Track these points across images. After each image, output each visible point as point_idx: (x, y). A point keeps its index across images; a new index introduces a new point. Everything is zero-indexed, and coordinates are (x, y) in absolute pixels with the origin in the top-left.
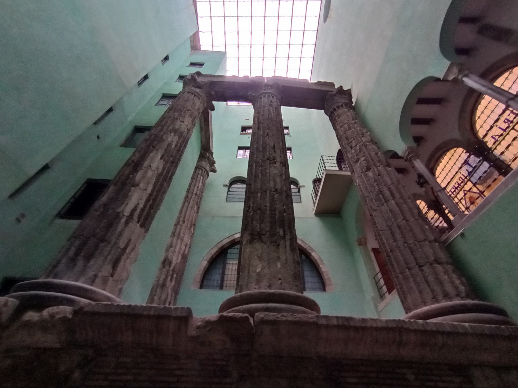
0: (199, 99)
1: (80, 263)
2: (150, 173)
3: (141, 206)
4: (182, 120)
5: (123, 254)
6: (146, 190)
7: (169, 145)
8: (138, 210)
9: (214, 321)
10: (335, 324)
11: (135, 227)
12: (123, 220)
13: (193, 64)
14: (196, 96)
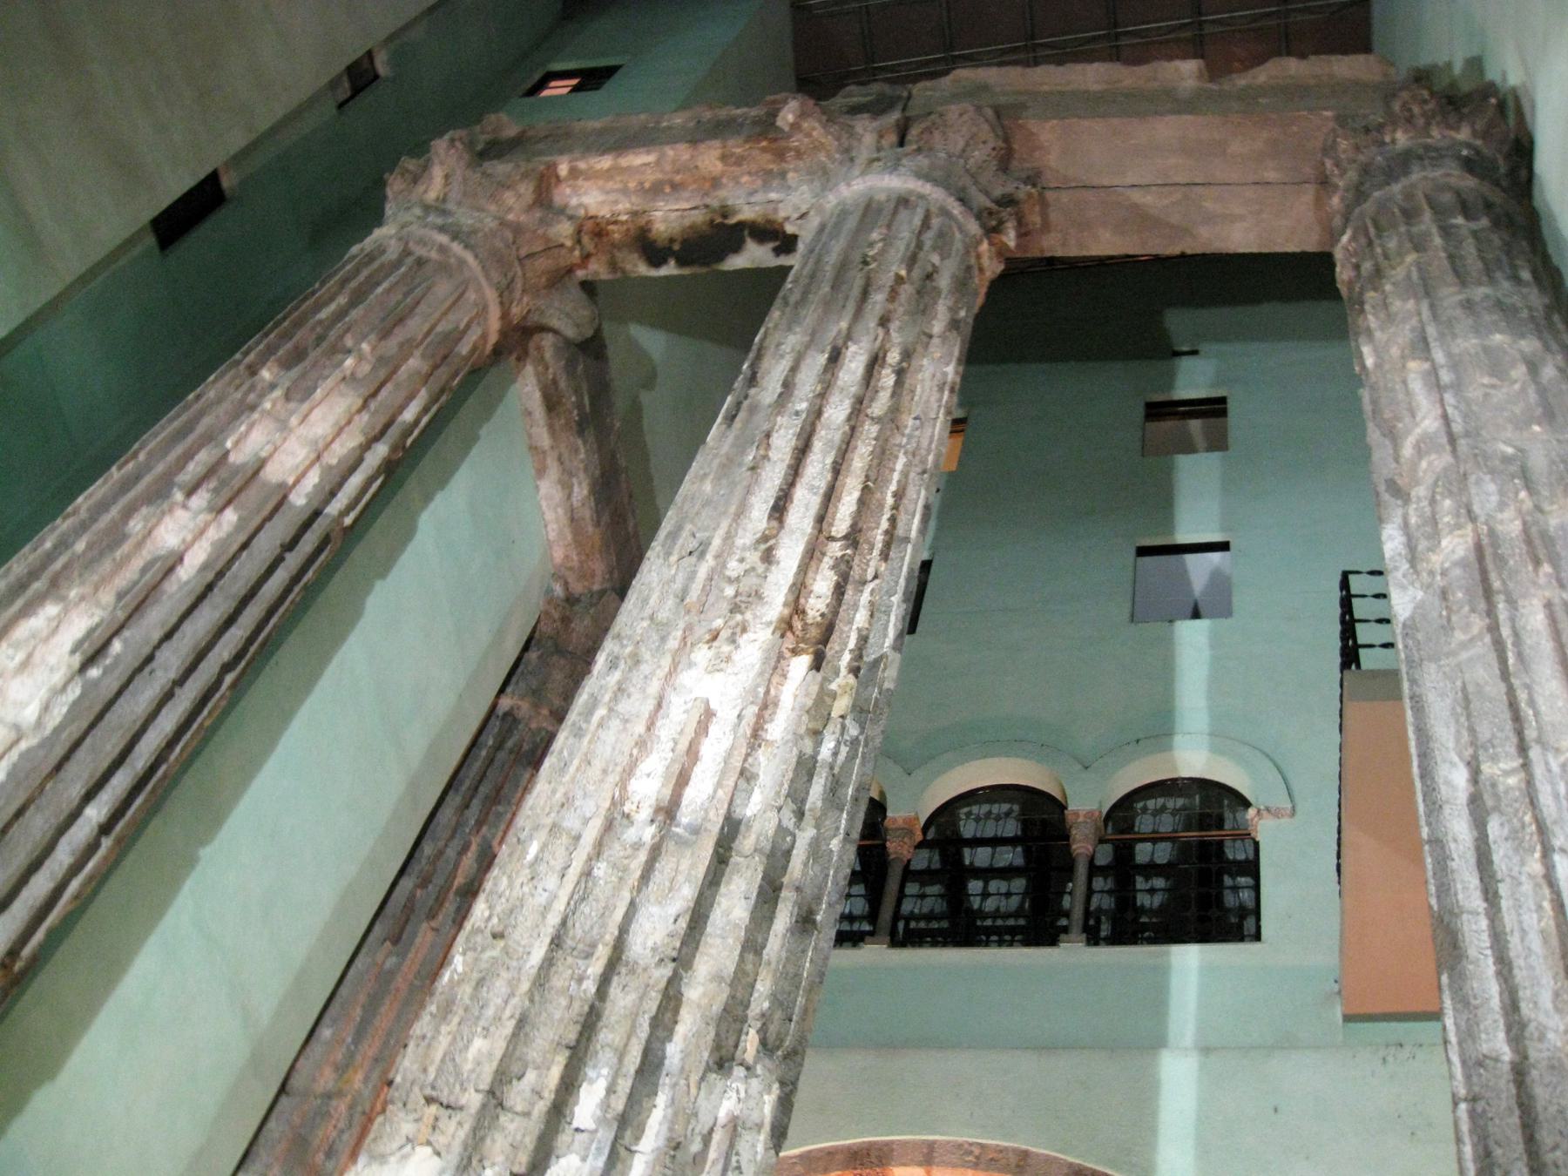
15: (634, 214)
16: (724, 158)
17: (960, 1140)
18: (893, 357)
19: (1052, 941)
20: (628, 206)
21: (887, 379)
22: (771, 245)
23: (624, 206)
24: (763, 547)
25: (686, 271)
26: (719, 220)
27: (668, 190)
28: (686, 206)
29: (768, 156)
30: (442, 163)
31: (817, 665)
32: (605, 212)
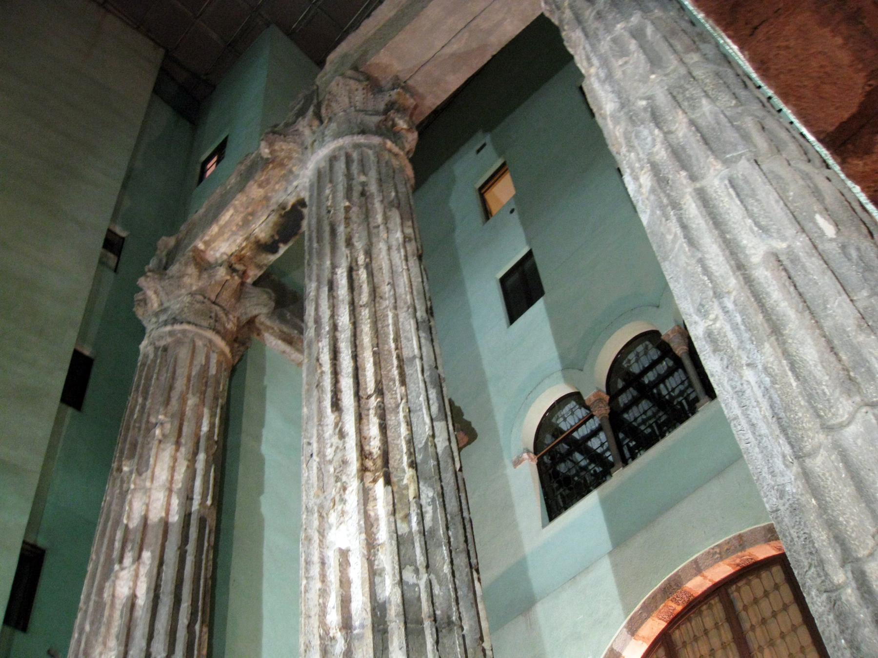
15: (247, 239)
16: (260, 186)
17: (707, 549)
18: (361, 259)
19: (693, 411)
20: (241, 238)
21: (363, 274)
23: (239, 239)
24: (337, 430)
25: (290, 244)
26: (283, 212)
27: (250, 218)
28: (264, 218)
29: (277, 170)
30: (149, 288)
31: (388, 482)
32: (234, 248)
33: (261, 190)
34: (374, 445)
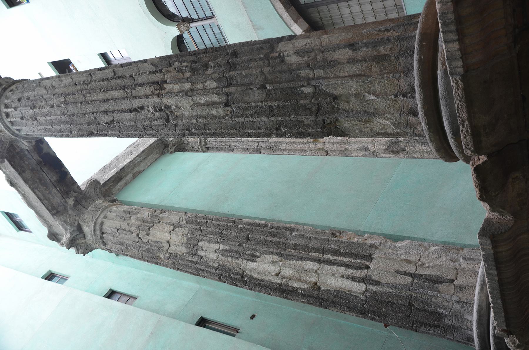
0: (102, 224)
1: (448, 322)
2: (287, 272)
3: (342, 269)
4: (166, 246)
5: (420, 276)
6: (316, 271)
7: (224, 253)
8: (350, 272)
9: (490, 206)
10: (458, 47)
11: (377, 268)
12: (374, 288)
13: (20, 226)
14: (101, 230)
15: (55, 187)
22: (41, 145)
23: (54, 190)
31: (166, 82)
33: (26, 172)
34: (148, 90)
